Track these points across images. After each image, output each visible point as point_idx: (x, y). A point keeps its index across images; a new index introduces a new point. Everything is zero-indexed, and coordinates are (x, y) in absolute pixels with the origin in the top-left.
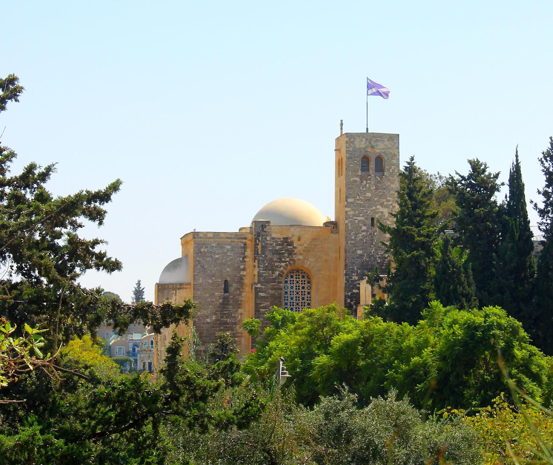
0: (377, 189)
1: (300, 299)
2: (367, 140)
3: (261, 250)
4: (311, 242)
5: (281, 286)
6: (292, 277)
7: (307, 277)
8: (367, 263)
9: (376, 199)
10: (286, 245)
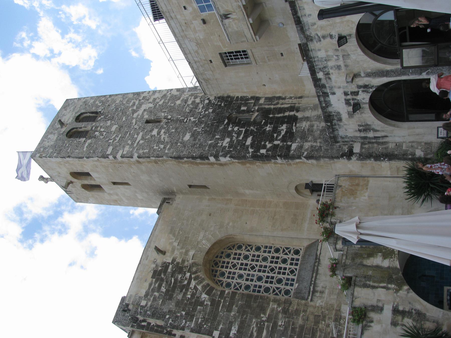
0: (112, 119)
1: (264, 264)
2: (51, 133)
3: (158, 318)
4: (174, 235)
5: (229, 293)
6: (223, 274)
7: (230, 249)
8: (208, 127)
9: (124, 119)
10: (165, 275)
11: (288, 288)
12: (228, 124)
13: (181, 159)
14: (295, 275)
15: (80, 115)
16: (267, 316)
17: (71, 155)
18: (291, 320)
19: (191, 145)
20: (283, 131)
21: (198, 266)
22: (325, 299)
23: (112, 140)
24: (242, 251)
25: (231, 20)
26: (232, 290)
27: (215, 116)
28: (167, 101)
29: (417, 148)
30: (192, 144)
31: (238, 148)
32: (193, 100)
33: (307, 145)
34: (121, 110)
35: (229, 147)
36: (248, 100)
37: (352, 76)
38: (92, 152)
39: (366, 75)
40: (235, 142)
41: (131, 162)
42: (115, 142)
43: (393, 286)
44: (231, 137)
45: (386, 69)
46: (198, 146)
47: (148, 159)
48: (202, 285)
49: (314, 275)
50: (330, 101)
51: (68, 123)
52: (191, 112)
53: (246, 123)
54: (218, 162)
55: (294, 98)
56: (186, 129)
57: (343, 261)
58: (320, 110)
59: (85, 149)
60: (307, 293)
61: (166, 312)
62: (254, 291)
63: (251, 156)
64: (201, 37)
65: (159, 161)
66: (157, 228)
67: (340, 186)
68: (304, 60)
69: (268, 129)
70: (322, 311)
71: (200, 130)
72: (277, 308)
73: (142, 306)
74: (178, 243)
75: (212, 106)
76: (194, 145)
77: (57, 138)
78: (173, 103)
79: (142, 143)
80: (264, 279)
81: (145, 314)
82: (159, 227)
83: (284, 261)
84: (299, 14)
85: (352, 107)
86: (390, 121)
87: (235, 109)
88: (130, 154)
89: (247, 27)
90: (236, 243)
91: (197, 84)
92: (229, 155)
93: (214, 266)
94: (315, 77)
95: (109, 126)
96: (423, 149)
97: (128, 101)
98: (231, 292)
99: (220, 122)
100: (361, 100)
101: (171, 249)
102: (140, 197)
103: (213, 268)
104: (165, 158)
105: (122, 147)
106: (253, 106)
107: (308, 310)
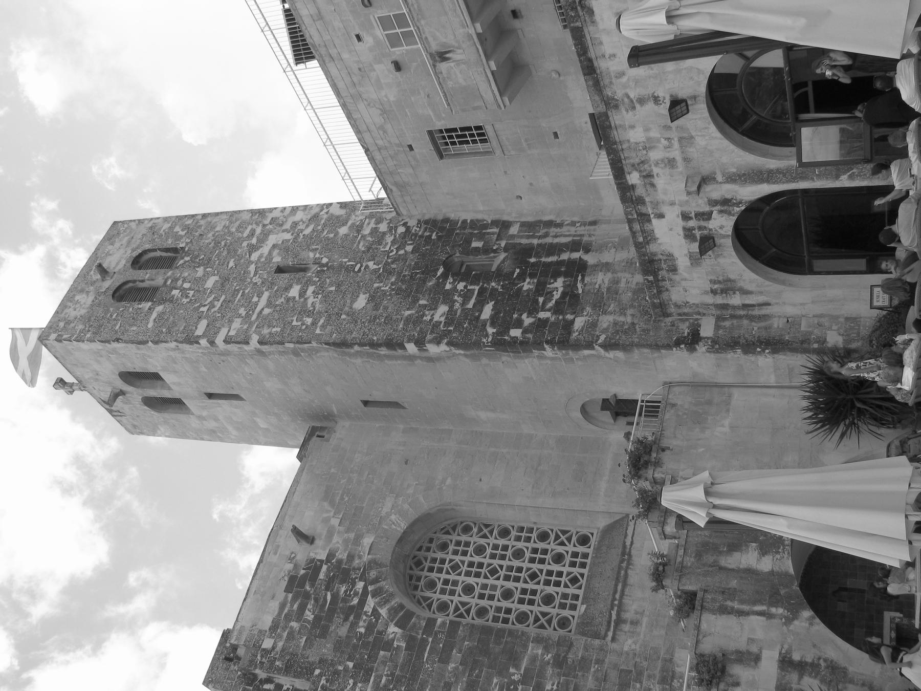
0: (207, 263)
1: (516, 563)
2: (82, 291)
3: (298, 675)
4: (332, 503)
5: (444, 623)
6: (432, 585)
7: (448, 533)
8: (403, 281)
9: (231, 264)
10: (312, 586)
11: (566, 613)
12: (445, 276)
13: (348, 348)
14: (580, 588)
15: (140, 255)
16: (522, 672)
17: (121, 337)
18: (572, 681)
19: (368, 318)
20: (557, 291)
21: (381, 567)
22: (642, 636)
23: (207, 307)
24: (472, 536)
25: (452, 64)
26: (451, 617)
27: (418, 259)
28: (319, 228)
29: (830, 328)
30: (371, 316)
31: (465, 326)
32: (374, 226)
33: (606, 321)
34: (225, 245)
35: (447, 324)
36: (486, 226)
37: (698, 180)
38: (164, 330)
39: (727, 179)
40: (458, 314)
41: (246, 353)
42: (213, 310)
43: (780, 611)
44: (451, 303)
45: (767, 166)
46: (383, 320)
47: (280, 348)
48: (387, 607)
49: (620, 587)
50: (653, 231)
51: (116, 270)
52: (368, 251)
53: (481, 274)
54: (424, 354)
55: (579, 224)
56: (359, 287)
57: (679, 559)
58: (633, 249)
59: (150, 325)
60: (605, 623)
61: (314, 663)
62: (496, 619)
63: (491, 342)
64: (392, 99)
65: (303, 350)
66: (298, 488)
67: (674, 405)
68: (600, 147)
69: (525, 288)
70: (634, 662)
71: (387, 288)
72: (543, 655)
73: (264, 650)
74: (339, 520)
75: (412, 240)
76: (375, 318)
77: (93, 301)
78: (332, 233)
79: (269, 314)
80: (517, 596)
81: (271, 667)
82: (301, 488)
83: (558, 559)
84: (592, 54)
85: (697, 244)
86: (775, 272)
87: (460, 246)
88: (243, 337)
89: (484, 78)
90: (460, 520)
91: (383, 195)
92: (446, 341)
93: (414, 567)
94: (622, 183)
95: (200, 278)
96: (842, 331)
97: (241, 228)
98: (448, 622)
99: (429, 271)
100: (717, 229)
101: (325, 533)
102: (263, 425)
103: (411, 572)
104: (314, 344)
105: (226, 321)
106: (497, 240)
107: (607, 660)
